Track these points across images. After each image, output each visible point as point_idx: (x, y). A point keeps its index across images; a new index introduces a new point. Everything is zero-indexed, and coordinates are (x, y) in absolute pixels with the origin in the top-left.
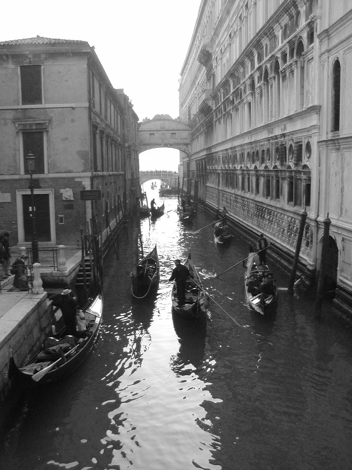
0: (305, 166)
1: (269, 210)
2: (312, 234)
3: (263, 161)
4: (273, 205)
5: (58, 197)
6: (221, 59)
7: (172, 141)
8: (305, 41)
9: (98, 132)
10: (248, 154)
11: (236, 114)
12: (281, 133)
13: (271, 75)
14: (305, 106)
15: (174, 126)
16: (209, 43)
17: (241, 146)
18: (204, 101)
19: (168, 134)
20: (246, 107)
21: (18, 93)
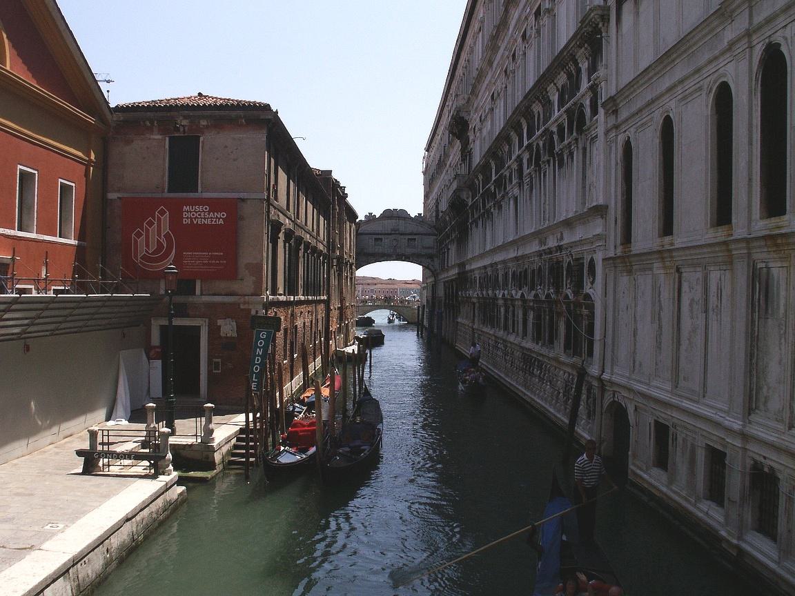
0: (588, 297)
1: (539, 361)
2: (595, 400)
3: (532, 288)
4: (544, 353)
5: (214, 331)
6: (480, 130)
7: (409, 251)
8: (588, 111)
9: (281, 235)
10: (514, 274)
11: (498, 213)
12: (556, 245)
13: (545, 158)
14: (587, 205)
15: (411, 228)
16: (464, 105)
17: (504, 262)
18: (454, 192)
19: (404, 240)
20: (512, 202)
21: (163, 176)
